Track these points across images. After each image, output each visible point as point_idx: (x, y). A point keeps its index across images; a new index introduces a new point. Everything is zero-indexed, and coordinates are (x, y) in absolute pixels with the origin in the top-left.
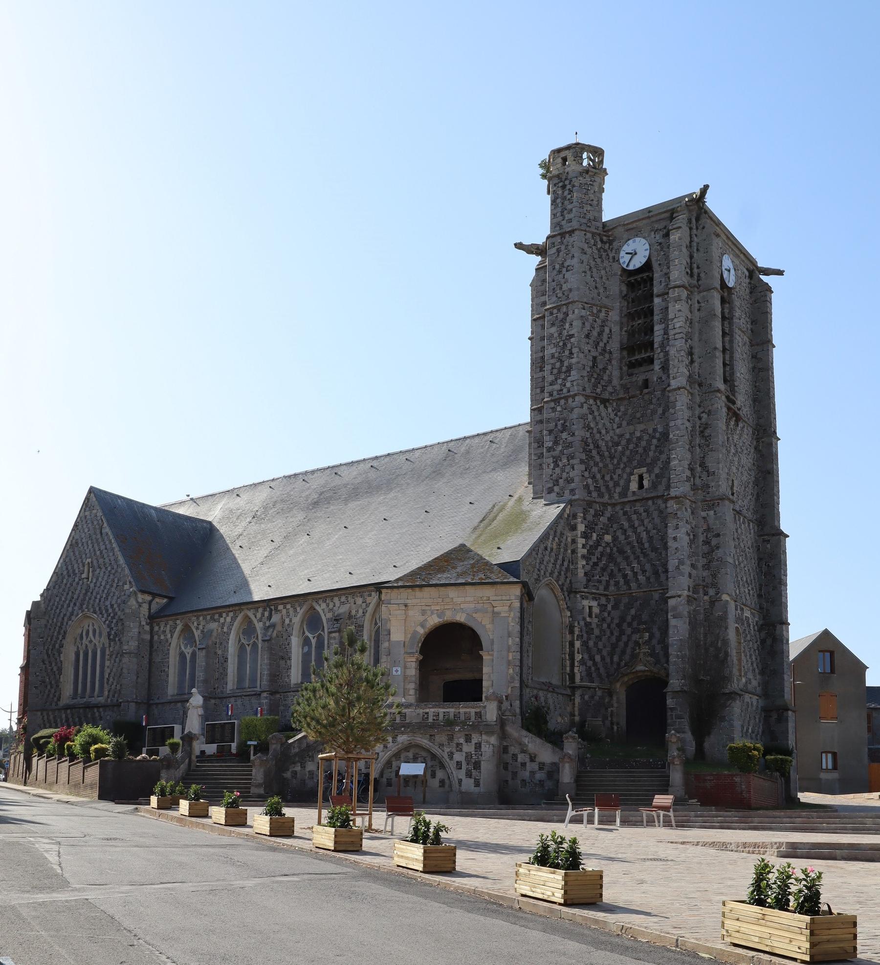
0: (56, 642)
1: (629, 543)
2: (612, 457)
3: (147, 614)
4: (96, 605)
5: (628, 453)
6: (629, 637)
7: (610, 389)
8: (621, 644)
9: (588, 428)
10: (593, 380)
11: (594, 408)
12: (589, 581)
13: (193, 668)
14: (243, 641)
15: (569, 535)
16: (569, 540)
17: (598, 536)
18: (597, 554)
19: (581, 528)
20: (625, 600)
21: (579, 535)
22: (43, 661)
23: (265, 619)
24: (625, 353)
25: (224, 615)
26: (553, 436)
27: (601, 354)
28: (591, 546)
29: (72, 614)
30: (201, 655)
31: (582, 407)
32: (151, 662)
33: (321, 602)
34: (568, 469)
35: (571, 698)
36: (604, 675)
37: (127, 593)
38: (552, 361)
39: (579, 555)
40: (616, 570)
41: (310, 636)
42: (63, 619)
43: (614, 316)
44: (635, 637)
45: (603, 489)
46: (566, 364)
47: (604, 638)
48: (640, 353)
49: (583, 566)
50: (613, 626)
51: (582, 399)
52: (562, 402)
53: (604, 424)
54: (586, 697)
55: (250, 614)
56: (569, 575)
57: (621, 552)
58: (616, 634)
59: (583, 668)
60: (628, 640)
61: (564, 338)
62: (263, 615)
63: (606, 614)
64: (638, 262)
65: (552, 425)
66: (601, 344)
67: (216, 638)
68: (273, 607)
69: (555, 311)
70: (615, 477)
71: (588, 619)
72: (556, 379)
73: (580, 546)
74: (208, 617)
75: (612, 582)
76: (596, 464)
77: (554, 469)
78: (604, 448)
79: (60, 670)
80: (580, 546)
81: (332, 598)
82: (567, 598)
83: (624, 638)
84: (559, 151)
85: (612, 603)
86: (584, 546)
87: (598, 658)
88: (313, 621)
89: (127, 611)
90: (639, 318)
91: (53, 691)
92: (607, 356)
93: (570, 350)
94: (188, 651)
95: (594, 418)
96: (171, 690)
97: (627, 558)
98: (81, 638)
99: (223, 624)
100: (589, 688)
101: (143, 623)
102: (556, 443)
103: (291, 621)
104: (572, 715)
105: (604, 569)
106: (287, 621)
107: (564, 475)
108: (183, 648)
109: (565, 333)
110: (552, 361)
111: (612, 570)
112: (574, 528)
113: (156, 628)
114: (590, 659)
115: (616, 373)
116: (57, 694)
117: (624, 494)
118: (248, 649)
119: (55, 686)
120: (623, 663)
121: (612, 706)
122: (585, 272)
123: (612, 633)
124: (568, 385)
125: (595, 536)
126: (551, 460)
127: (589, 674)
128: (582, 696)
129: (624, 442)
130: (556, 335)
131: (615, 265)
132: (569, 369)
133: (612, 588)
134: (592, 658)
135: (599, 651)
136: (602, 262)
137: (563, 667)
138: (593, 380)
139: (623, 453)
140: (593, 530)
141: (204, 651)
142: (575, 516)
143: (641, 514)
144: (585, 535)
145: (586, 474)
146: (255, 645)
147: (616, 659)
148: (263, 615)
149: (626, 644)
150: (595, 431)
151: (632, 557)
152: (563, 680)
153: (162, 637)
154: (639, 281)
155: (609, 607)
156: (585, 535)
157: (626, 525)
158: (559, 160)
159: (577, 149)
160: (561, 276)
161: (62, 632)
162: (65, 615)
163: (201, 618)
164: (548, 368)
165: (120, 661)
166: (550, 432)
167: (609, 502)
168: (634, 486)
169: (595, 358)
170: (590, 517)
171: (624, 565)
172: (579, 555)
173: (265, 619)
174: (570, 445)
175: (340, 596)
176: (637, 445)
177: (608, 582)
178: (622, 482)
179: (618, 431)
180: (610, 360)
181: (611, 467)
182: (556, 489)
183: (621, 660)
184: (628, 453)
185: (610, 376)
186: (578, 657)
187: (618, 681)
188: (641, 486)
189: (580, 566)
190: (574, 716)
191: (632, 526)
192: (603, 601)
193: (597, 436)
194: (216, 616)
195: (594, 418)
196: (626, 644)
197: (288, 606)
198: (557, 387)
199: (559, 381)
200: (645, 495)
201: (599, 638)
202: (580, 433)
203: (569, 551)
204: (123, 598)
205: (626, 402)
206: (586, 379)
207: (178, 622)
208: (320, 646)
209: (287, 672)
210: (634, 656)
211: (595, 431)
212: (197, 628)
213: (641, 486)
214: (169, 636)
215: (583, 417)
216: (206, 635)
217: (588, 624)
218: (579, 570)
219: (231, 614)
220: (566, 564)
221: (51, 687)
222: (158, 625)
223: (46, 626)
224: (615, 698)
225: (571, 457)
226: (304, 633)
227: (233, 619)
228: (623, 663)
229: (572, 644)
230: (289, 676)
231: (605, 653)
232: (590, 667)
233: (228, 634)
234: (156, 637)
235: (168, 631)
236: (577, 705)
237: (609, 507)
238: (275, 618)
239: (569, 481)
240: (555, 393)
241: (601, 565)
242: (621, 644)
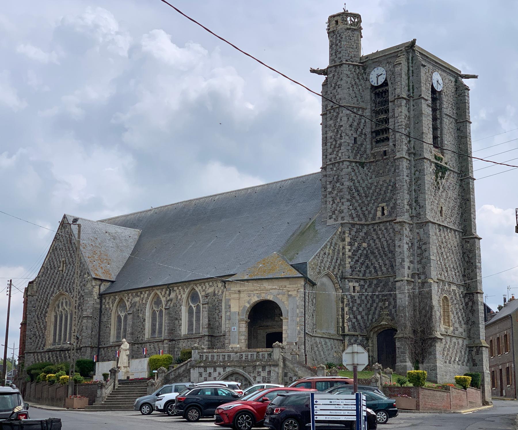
0: (43, 309)
1: (377, 248)
2: (366, 197)
3: (98, 292)
4: (67, 287)
5: (376, 194)
7: (365, 156)
8: (373, 308)
9: (352, 180)
10: (354, 151)
11: (355, 168)
12: (353, 271)
13: (125, 325)
14: (154, 308)
15: (341, 244)
16: (341, 247)
17: (358, 244)
18: (358, 254)
19: (348, 240)
20: (375, 282)
21: (347, 244)
22: (35, 322)
23: (166, 296)
24: (374, 135)
25: (143, 293)
26: (332, 185)
27: (359, 136)
28: (354, 251)
29: (53, 292)
30: (130, 317)
31: (348, 168)
32: (100, 322)
33: (198, 285)
34: (340, 204)
37: (86, 279)
38: (331, 141)
39: (347, 256)
40: (370, 264)
41: (193, 305)
42: (47, 295)
43: (368, 113)
44: (380, 304)
45: (361, 216)
46: (338, 142)
47: (363, 305)
48: (383, 134)
49: (350, 263)
50: (368, 297)
51: (348, 163)
52: (337, 165)
53: (362, 177)
55: (158, 292)
56: (341, 268)
57: (373, 253)
58: (370, 302)
61: (337, 127)
62: (166, 293)
63: (364, 291)
64: (381, 80)
65: (331, 179)
66: (360, 130)
67: (139, 307)
68: (171, 289)
69: (332, 111)
70: (369, 208)
71: (353, 294)
72: (333, 151)
73: (347, 250)
74: (134, 294)
75: (368, 271)
76: (357, 201)
77: (332, 205)
78: (362, 191)
79: (45, 327)
80: (347, 250)
81: (204, 283)
82: (340, 282)
83: (375, 305)
84: (334, 16)
85: (368, 284)
86: (350, 251)
87: (359, 317)
88: (194, 297)
89: (86, 291)
90: (382, 114)
91: (41, 340)
92: (363, 136)
93: (341, 134)
94: (122, 315)
95: (356, 174)
96: (112, 339)
97: (375, 257)
98: (59, 307)
99: (143, 298)
100: (354, 335)
101: (96, 298)
102: (333, 189)
103: (181, 297)
105: (362, 264)
106: (179, 297)
107: (338, 209)
108: (119, 313)
109: (338, 124)
110: (331, 141)
111: (368, 264)
112: (343, 240)
113: (104, 301)
114: (354, 318)
115: (369, 146)
116: (43, 343)
117: (373, 219)
118: (157, 313)
119: (42, 337)
120: (374, 320)
122: (349, 88)
123: (368, 302)
124: (340, 155)
125: (356, 244)
126: (331, 199)
127: (354, 327)
129: (373, 188)
130: (333, 125)
131: (367, 82)
132: (340, 145)
133: (367, 275)
134: (355, 317)
135: (360, 313)
136: (360, 81)
138: (354, 151)
139: (373, 194)
140: (355, 240)
141: (131, 315)
142: (344, 233)
143: (383, 231)
144: (350, 244)
145: (351, 207)
146: (161, 311)
147: (370, 317)
148: (166, 293)
149: (376, 309)
150: (356, 181)
151: (378, 256)
152: (338, 331)
153: (107, 306)
154: (381, 92)
155: (366, 286)
156: (350, 244)
157: (375, 237)
158: (334, 22)
159: (345, 14)
160: (335, 90)
161: (47, 303)
162: (48, 293)
163: (130, 295)
164: (329, 144)
165: (82, 321)
166: (330, 182)
167: (365, 223)
168: (379, 214)
169: (355, 139)
170: (353, 233)
171: (374, 261)
172: (347, 256)
173: (166, 296)
174: (341, 191)
175: (209, 282)
176: (381, 190)
177: (365, 271)
178: (373, 212)
179: (370, 181)
180: (365, 139)
181: (366, 202)
182: (334, 216)
183: (373, 318)
184: (376, 194)
185: (366, 148)
186: (347, 317)
187: (371, 330)
188: (383, 214)
189: (347, 262)
191: (378, 238)
192: (362, 282)
193: (357, 185)
194: (139, 294)
195: (356, 174)
196: (376, 309)
197: (180, 288)
198: (333, 156)
199: (335, 153)
200: (385, 220)
201: (360, 305)
202: (347, 183)
203: (341, 254)
204: (84, 282)
205: (374, 164)
206: (350, 151)
207: (117, 297)
208: (198, 312)
209: (179, 328)
210: (379, 315)
211: (356, 181)
212: (128, 301)
213: (383, 214)
214: (111, 305)
215: (349, 174)
216: (133, 305)
217: (352, 297)
218: (347, 265)
219: (147, 292)
220: (339, 262)
221: (40, 338)
222: (105, 298)
223: (37, 300)
224: (370, 341)
225: (342, 198)
226: (189, 304)
227: (149, 295)
228: (374, 320)
229: (343, 309)
230: (180, 330)
231: (363, 313)
232: (354, 323)
233: (146, 304)
234: (103, 306)
235: (110, 303)
237: (365, 227)
238: (173, 295)
239: (341, 212)
240: (333, 160)
241: (361, 261)
242: (373, 308)
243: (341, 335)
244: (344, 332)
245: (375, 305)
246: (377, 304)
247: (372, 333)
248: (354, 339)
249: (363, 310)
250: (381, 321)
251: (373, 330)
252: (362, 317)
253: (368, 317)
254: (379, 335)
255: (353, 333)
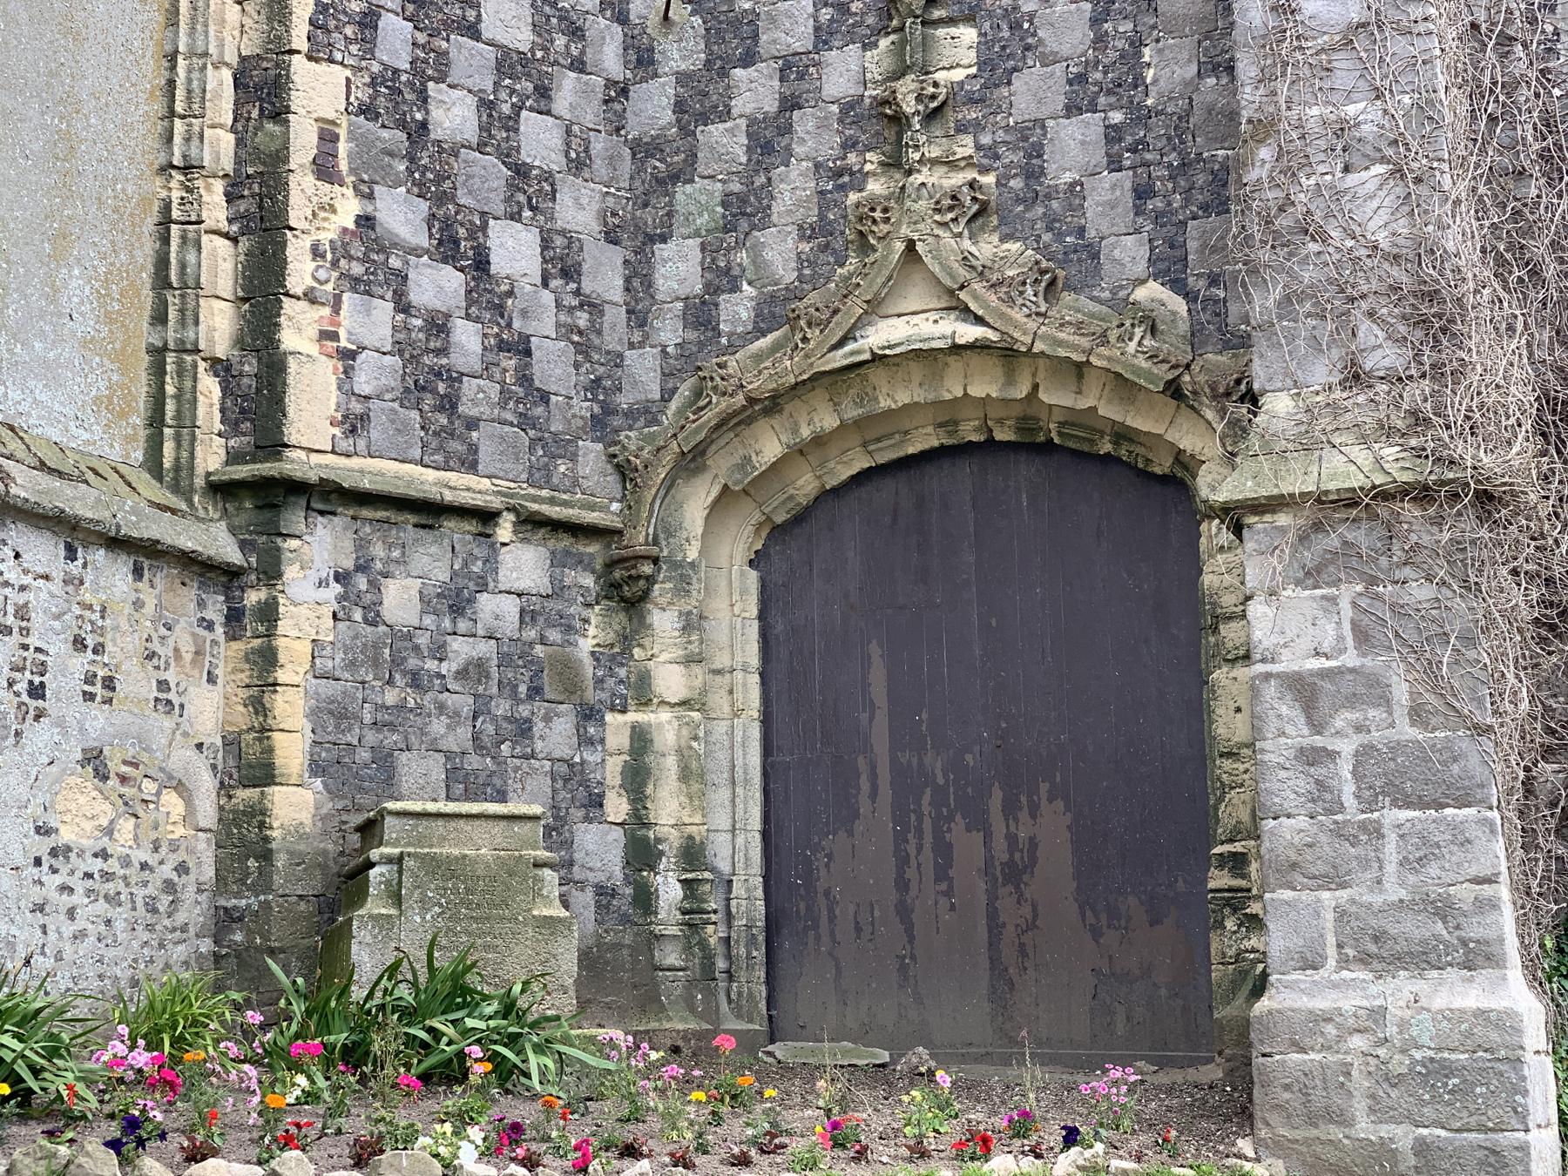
6: (796, 71)
8: (725, 142)
35: (237, 591)
36: (571, 405)
47: (567, 89)
54: (400, 600)
59: (370, 321)
60: (790, 104)
83: (755, 90)
87: (514, 250)
104: (249, 766)
114: (447, 248)
120: (737, 309)
121: (642, 692)
123: (643, 60)
127: (429, 383)
128: (356, 586)
135: (529, 191)
137: (170, 285)
152: (162, 419)
183: (721, 279)
186: (318, 213)
187: (692, 461)
190: (263, 774)
196: (768, 142)
210: (841, 233)
224: (663, 621)
228: (737, 309)
229: (263, 90)
232: (438, 325)
236: (293, 668)
242: (725, 142)
243: (221, 490)
244: (273, 446)
245: (755, 90)
246: (793, 68)
247: (696, 502)
248: (431, 559)
249: (578, 165)
250: (875, 309)
251: (721, 465)
252: (562, 264)
253: (639, 277)
254: (787, 549)
255: (427, 480)
